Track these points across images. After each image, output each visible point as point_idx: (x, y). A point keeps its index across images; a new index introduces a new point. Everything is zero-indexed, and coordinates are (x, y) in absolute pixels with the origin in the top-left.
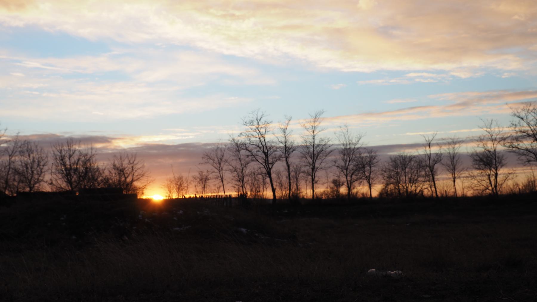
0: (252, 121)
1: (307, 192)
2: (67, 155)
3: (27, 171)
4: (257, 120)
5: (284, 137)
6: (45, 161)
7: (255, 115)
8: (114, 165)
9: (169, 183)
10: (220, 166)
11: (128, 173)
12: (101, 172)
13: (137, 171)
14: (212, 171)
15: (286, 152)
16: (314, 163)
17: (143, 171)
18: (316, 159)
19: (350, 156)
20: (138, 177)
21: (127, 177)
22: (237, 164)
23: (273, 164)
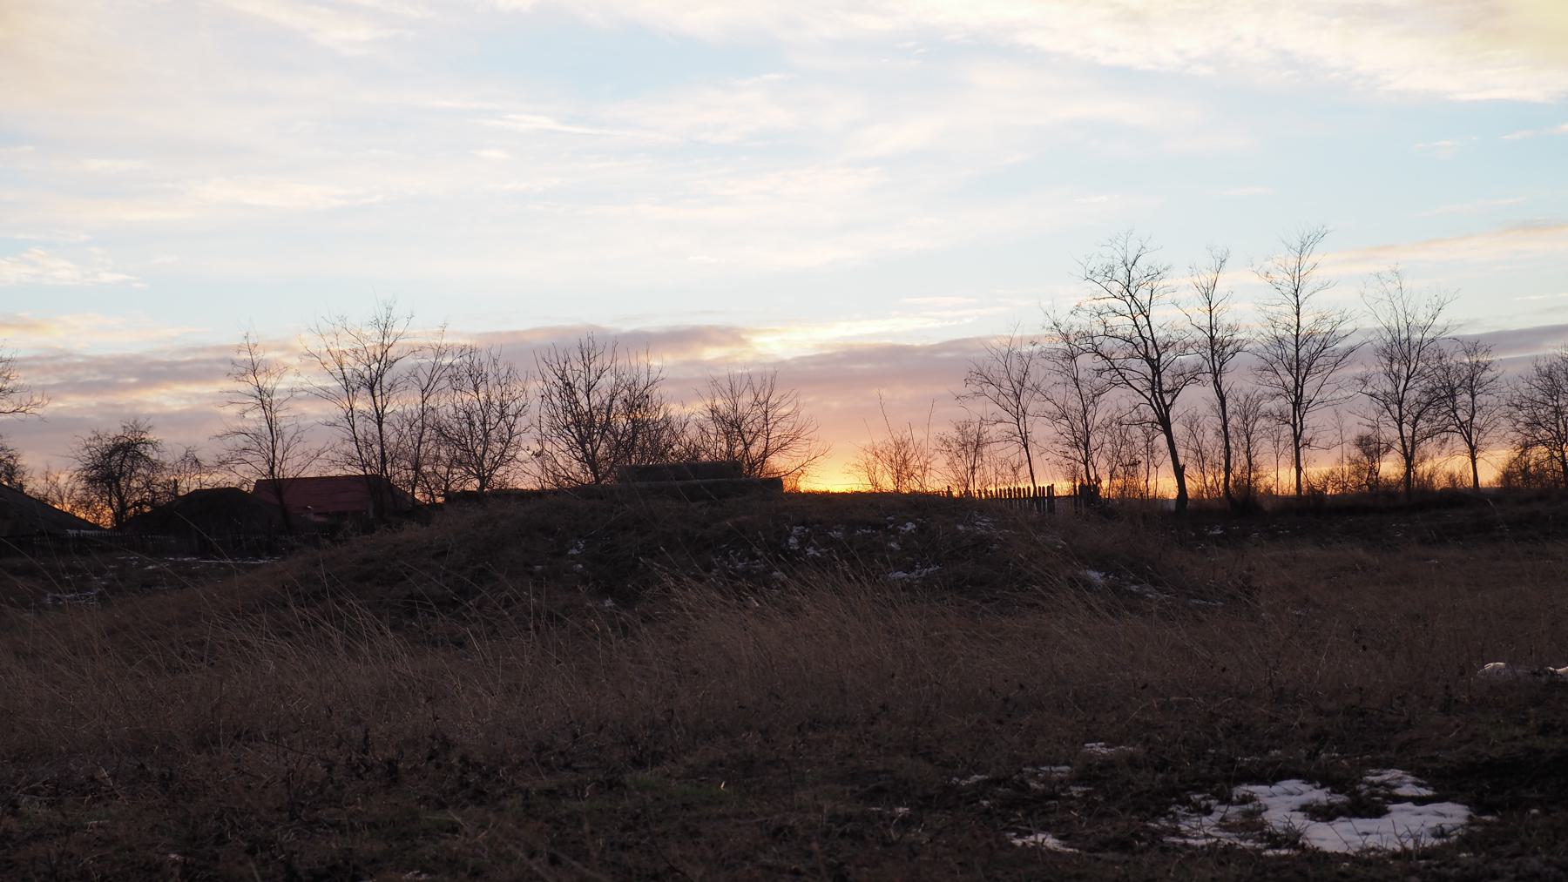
1: (1278, 477)
3: (471, 433)
7: (1119, 249)
9: (871, 457)
12: (678, 429)
13: (779, 424)
15: (1213, 355)
16: (1298, 386)
17: (795, 423)
19: (1409, 362)
21: (751, 443)
22: (1068, 394)
23: (1175, 392)
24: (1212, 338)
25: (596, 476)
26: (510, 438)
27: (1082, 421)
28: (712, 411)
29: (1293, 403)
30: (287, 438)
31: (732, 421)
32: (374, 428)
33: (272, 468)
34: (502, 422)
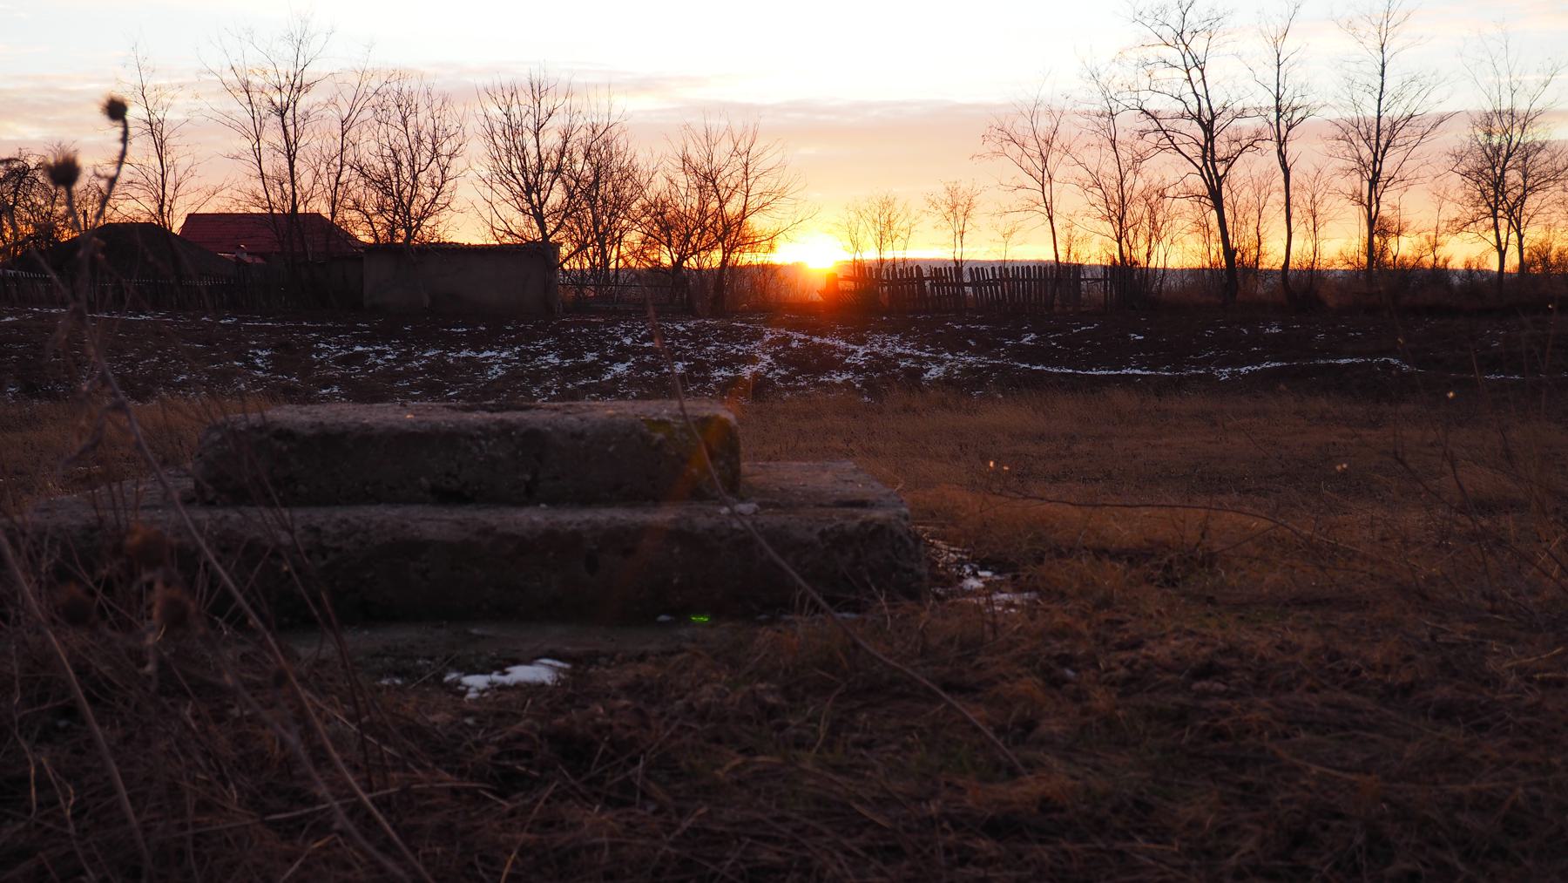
0: (1164, 10)
2: (530, 122)
6: (454, 142)
10: (1046, 166)
11: (732, 185)
12: (644, 180)
13: (762, 179)
14: (1018, 183)
18: (1387, 146)
20: (765, 199)
22: (1103, 158)
23: (1229, 161)
24: (1278, 99)
26: (443, 182)
27: (1118, 191)
28: (684, 160)
29: (1369, 180)
30: (180, 172)
31: (706, 174)
32: (284, 162)
33: (161, 207)
34: (434, 164)
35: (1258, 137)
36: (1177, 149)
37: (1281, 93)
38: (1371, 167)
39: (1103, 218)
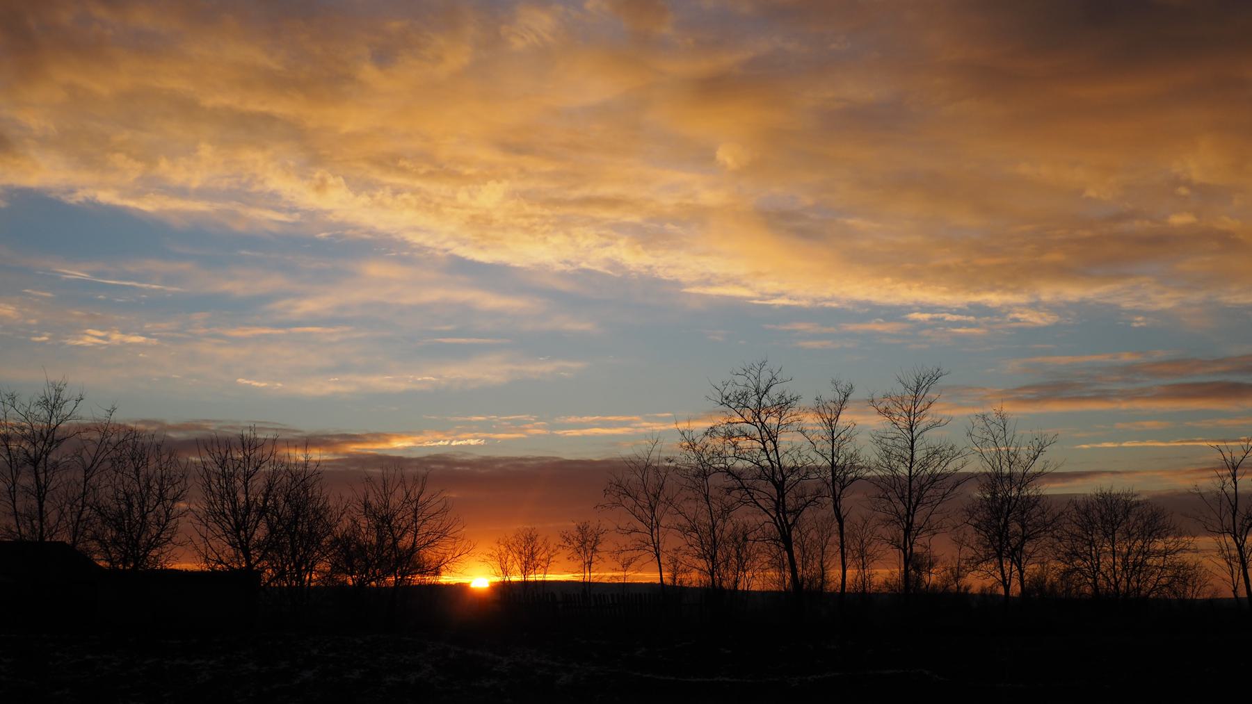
0: (744, 395)
4: (758, 394)
5: (831, 442)
7: (752, 378)
8: (367, 505)
10: (654, 515)
11: (403, 525)
13: (428, 522)
14: (632, 527)
15: (834, 480)
16: (910, 513)
18: (917, 503)
22: (699, 509)
23: (797, 512)
25: (248, 561)
27: (710, 535)
28: (365, 506)
29: (904, 530)
32: (34, 502)
34: (159, 507)
35: (819, 493)
36: (756, 503)
37: (835, 461)
38: (905, 519)
39: (699, 557)
